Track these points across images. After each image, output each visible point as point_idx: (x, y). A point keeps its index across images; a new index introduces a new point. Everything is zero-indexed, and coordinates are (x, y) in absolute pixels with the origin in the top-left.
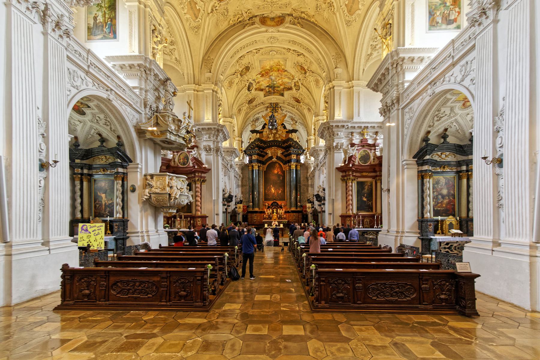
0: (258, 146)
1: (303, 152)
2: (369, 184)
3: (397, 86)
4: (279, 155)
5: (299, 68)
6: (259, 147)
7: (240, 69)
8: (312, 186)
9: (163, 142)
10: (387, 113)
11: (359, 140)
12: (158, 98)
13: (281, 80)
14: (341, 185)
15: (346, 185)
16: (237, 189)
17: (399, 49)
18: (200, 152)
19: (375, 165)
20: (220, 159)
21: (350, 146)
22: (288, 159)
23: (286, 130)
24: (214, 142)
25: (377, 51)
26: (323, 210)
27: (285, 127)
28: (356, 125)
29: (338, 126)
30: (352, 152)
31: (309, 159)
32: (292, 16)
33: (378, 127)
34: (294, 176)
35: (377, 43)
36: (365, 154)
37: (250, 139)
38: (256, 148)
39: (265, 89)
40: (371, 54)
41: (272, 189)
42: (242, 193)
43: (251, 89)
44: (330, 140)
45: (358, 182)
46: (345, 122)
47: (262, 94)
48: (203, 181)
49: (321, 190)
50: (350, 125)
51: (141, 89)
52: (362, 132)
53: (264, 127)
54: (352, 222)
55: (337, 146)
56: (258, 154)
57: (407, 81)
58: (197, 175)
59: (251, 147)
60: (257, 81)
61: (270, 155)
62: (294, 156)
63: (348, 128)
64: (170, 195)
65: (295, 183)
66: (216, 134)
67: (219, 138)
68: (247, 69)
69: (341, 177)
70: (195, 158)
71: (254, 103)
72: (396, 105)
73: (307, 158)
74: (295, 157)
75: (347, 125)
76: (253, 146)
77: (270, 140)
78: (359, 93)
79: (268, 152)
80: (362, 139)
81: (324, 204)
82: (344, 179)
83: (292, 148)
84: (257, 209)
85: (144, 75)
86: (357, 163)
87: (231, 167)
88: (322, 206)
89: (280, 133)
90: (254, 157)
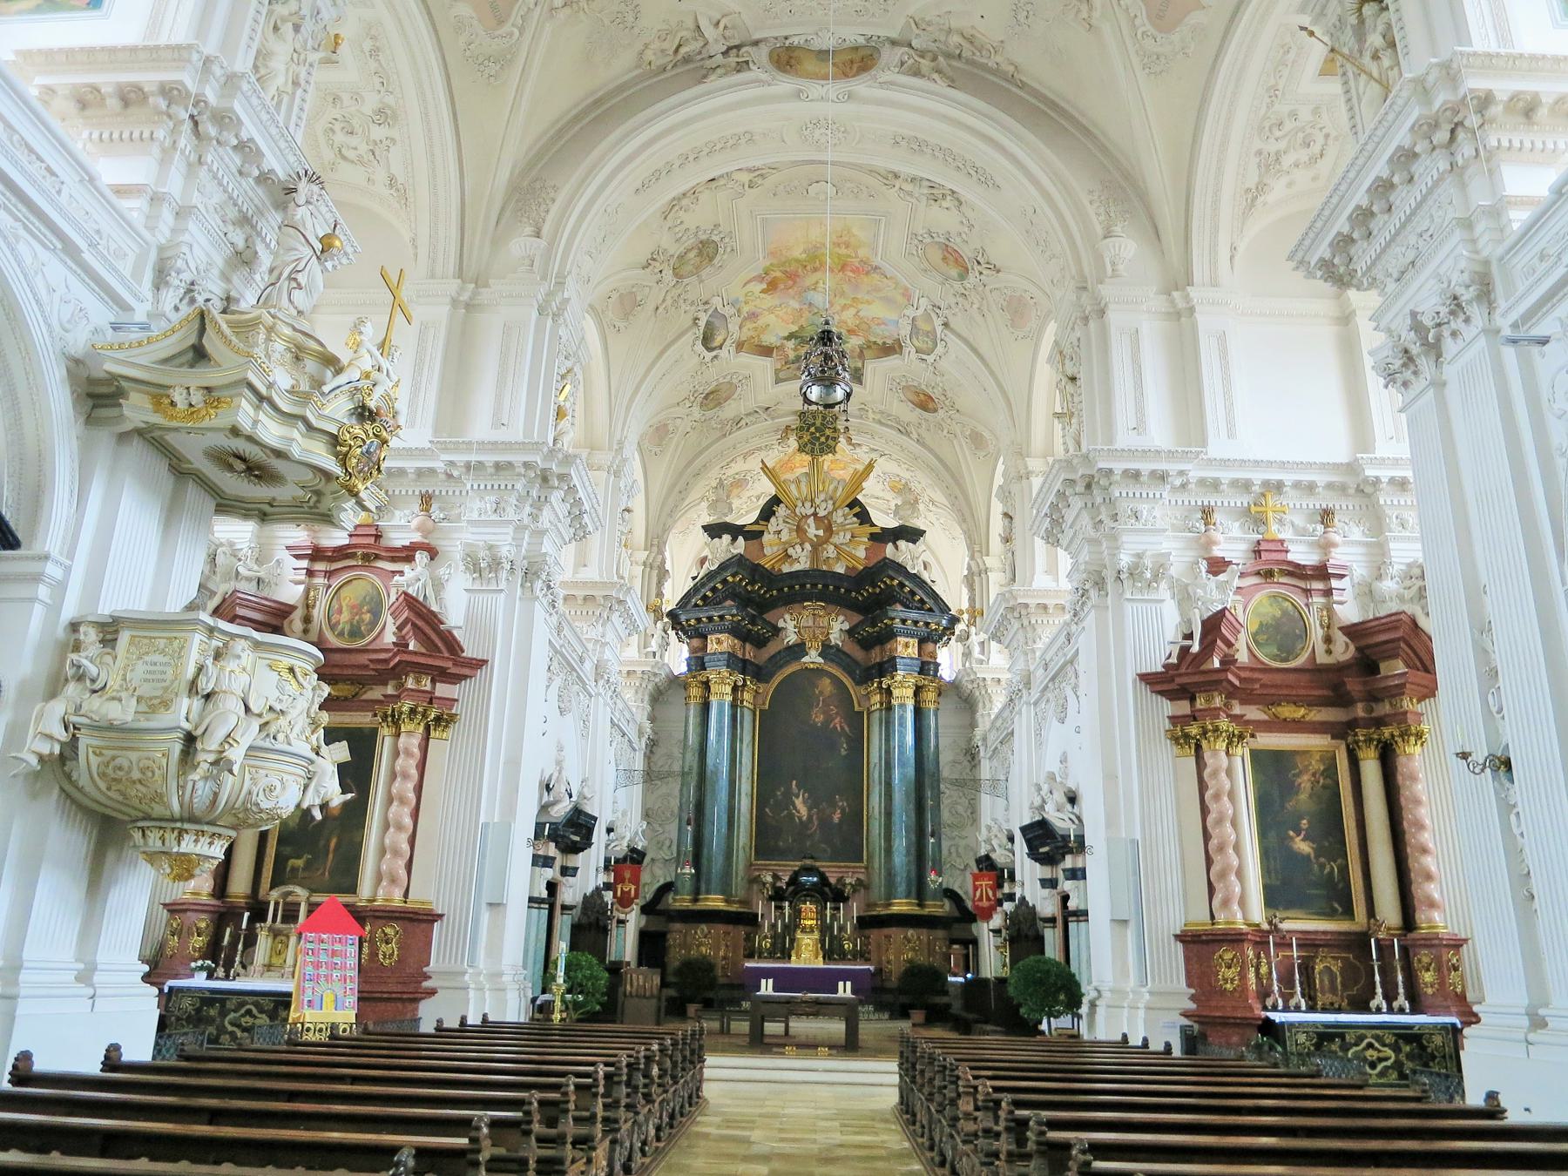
0: (733, 593)
1: (949, 629)
2: (1316, 765)
3: (1467, 224)
4: (835, 638)
5: (936, 255)
6: (744, 600)
7: (675, 250)
8: (999, 787)
9: (224, 459)
10: (1425, 364)
11: (1244, 546)
12: (243, 259)
13: (852, 311)
14: (1174, 766)
15: (1200, 764)
16: (621, 792)
17: (1461, 54)
18: (442, 571)
19: (1339, 669)
20: (539, 611)
21: (1204, 566)
22: (876, 656)
23: (868, 529)
24: (520, 528)
25: (1284, 180)
26: (1072, 905)
27: (864, 517)
28: (1226, 476)
29: (1136, 475)
30: (1216, 595)
31: (981, 662)
32: (910, 46)
33: (1330, 486)
34: (910, 739)
35: (1282, 145)
36: (1278, 613)
37: (703, 561)
38: (729, 603)
39: (781, 348)
40: (1261, 187)
41: (799, 802)
42: (647, 815)
43: (718, 340)
44: (1094, 542)
45: (1256, 756)
46: (1171, 455)
47: (763, 367)
48: (438, 719)
49: (1060, 797)
50: (1195, 474)
51: (156, 199)
52: (1253, 509)
53: (767, 513)
54: (1252, 975)
55: (1134, 572)
56: (735, 631)
57: (1522, 202)
58: (410, 683)
59: (705, 598)
60: (746, 309)
61: (791, 638)
62: (907, 645)
63: (1183, 486)
64: (190, 739)
65: (911, 771)
66: (534, 493)
67: (546, 515)
68: (707, 250)
69: (1168, 725)
70: (410, 602)
71: (730, 410)
72: (1476, 312)
73: (967, 655)
74: (913, 651)
75: (1181, 473)
76: (714, 589)
77: (797, 567)
78: (1222, 339)
79: (781, 624)
80: (1258, 542)
81: (1077, 874)
82: (1187, 736)
83: (899, 607)
84: (715, 902)
85: (185, 140)
86: (1242, 657)
87: (598, 675)
88: (1067, 886)
89: (841, 538)
90: (721, 643)
